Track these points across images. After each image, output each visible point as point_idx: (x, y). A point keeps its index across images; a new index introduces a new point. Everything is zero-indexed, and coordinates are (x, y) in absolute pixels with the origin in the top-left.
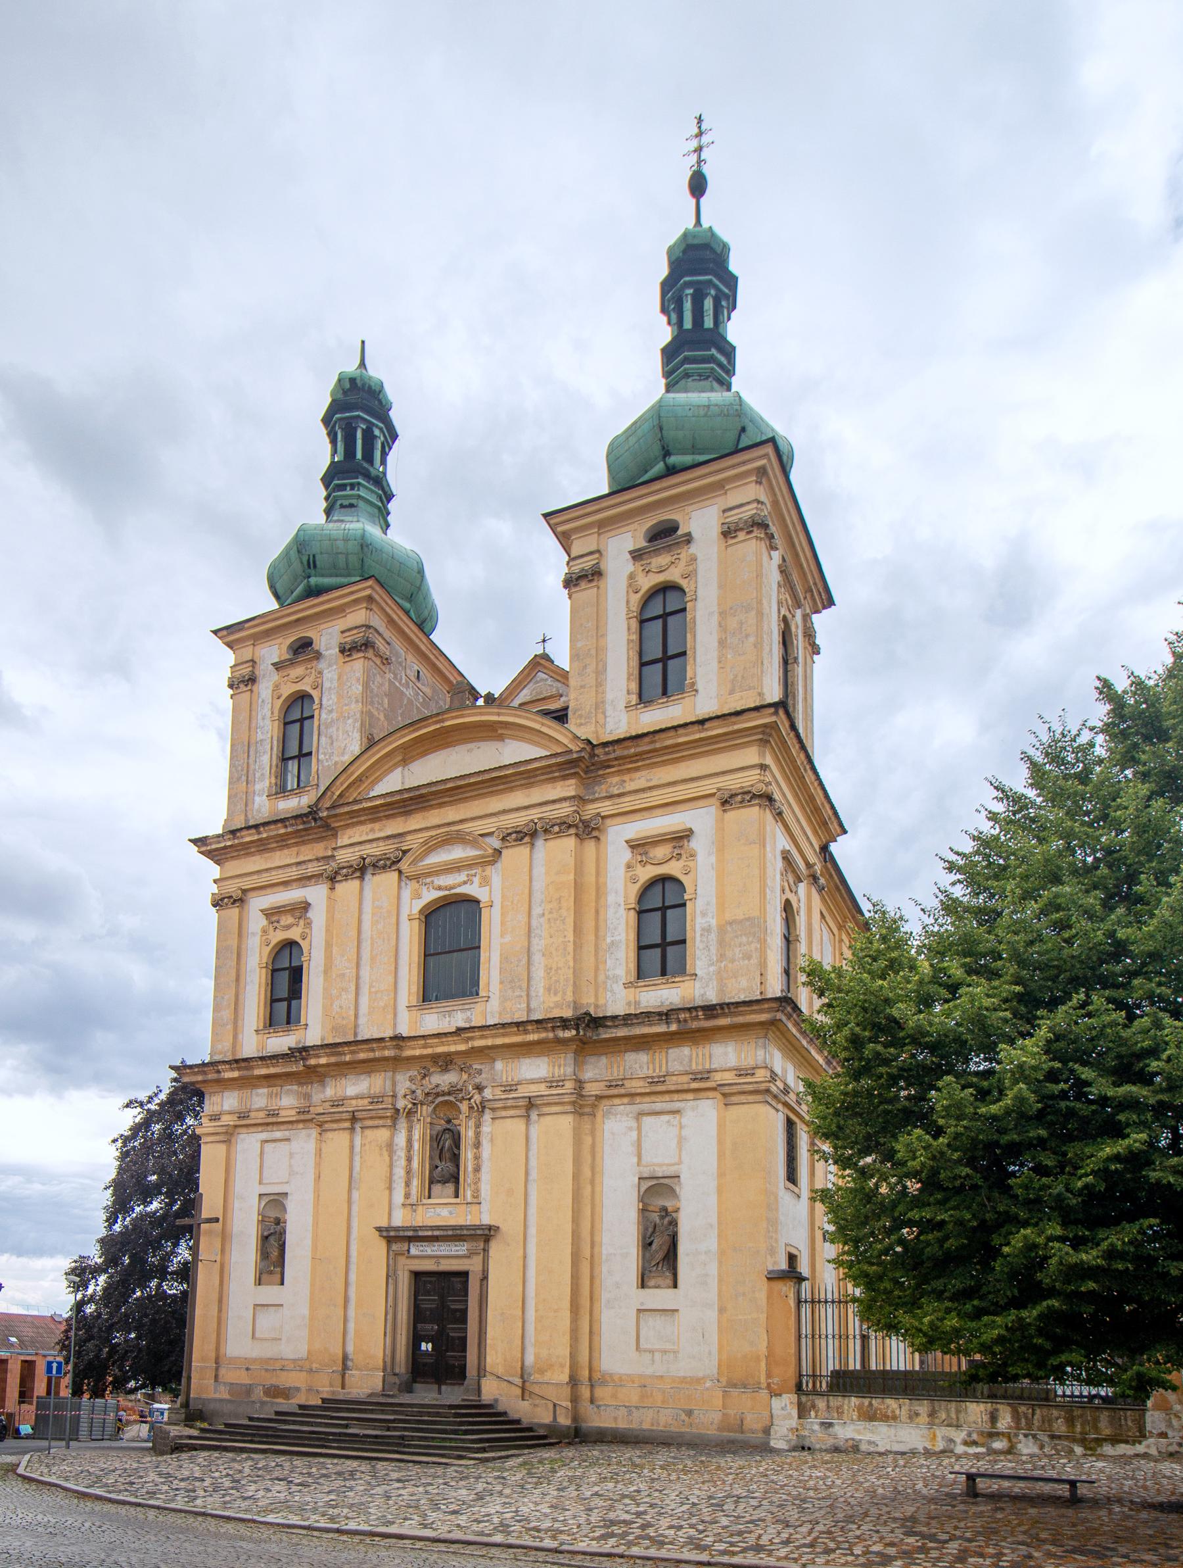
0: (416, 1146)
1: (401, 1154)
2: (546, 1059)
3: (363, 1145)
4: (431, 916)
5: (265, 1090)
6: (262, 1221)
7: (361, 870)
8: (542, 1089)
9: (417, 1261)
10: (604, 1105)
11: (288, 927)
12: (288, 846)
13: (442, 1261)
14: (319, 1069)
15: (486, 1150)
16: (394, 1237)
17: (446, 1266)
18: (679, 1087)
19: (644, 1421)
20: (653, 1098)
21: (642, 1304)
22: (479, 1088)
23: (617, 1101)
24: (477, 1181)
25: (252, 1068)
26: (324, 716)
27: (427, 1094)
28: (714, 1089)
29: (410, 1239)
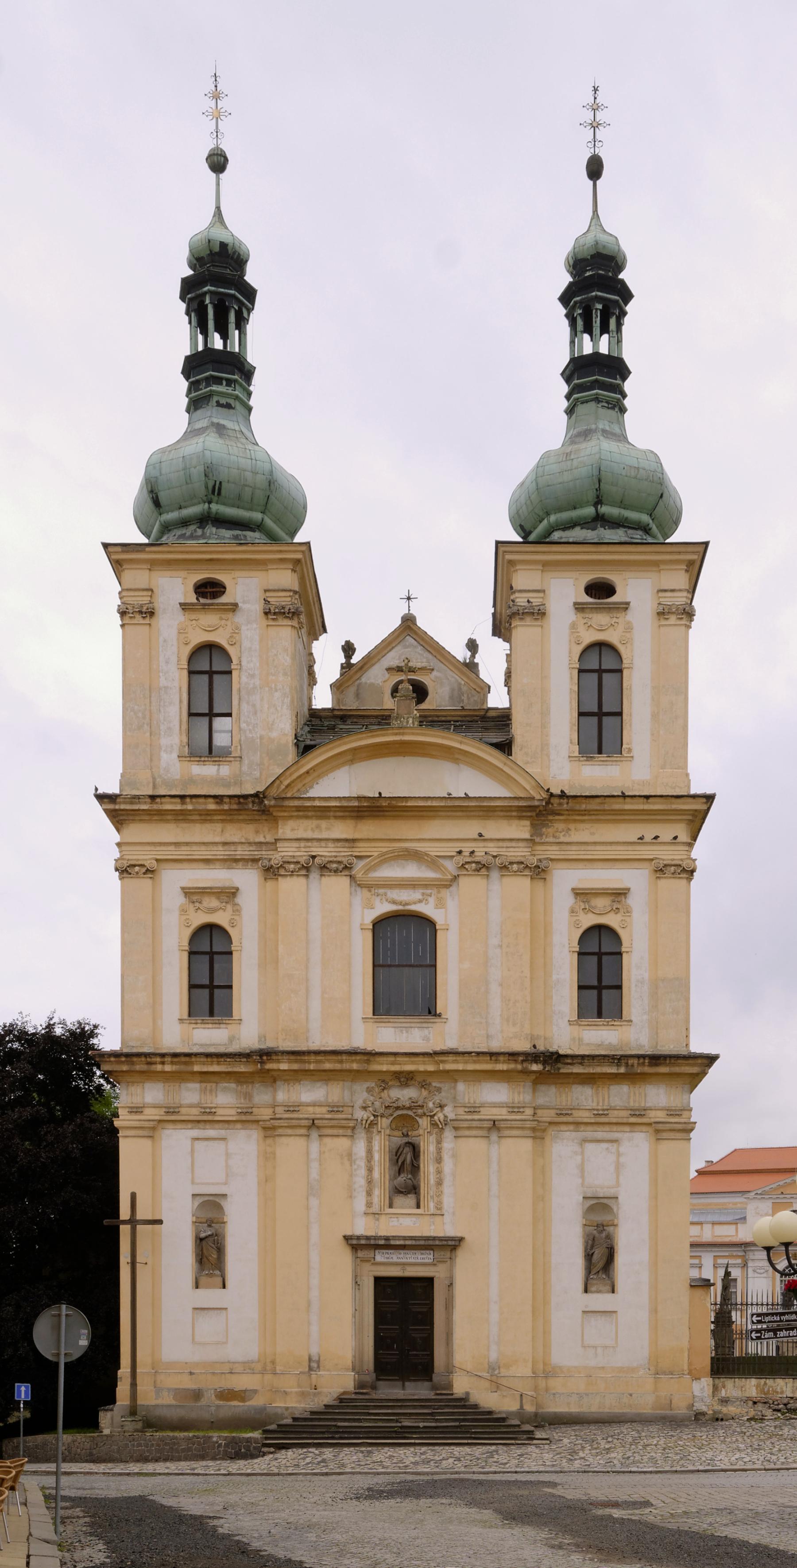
0: (376, 1156)
1: (362, 1163)
2: (505, 1085)
3: (321, 1153)
5: (197, 1085)
7: (306, 868)
8: (501, 1114)
9: (382, 1268)
10: (552, 1131)
11: (212, 911)
12: (211, 821)
13: (409, 1268)
14: (273, 1073)
15: (448, 1166)
17: (410, 1272)
18: (620, 1121)
19: (592, 1406)
20: (596, 1128)
21: (586, 1306)
22: (441, 1107)
23: (563, 1128)
24: (440, 1194)
25: (192, 1063)
26: (244, 679)
27: (387, 1107)
28: (650, 1124)
29: (377, 1247)
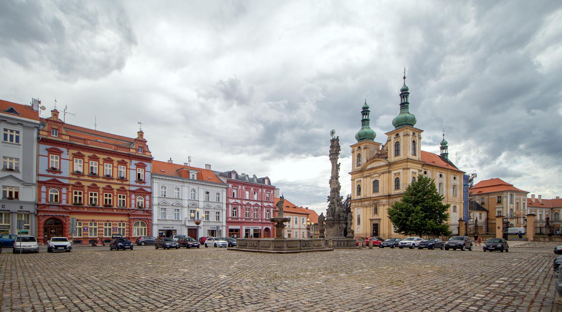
4: (374, 182)
7: (366, 177)
16: (371, 220)
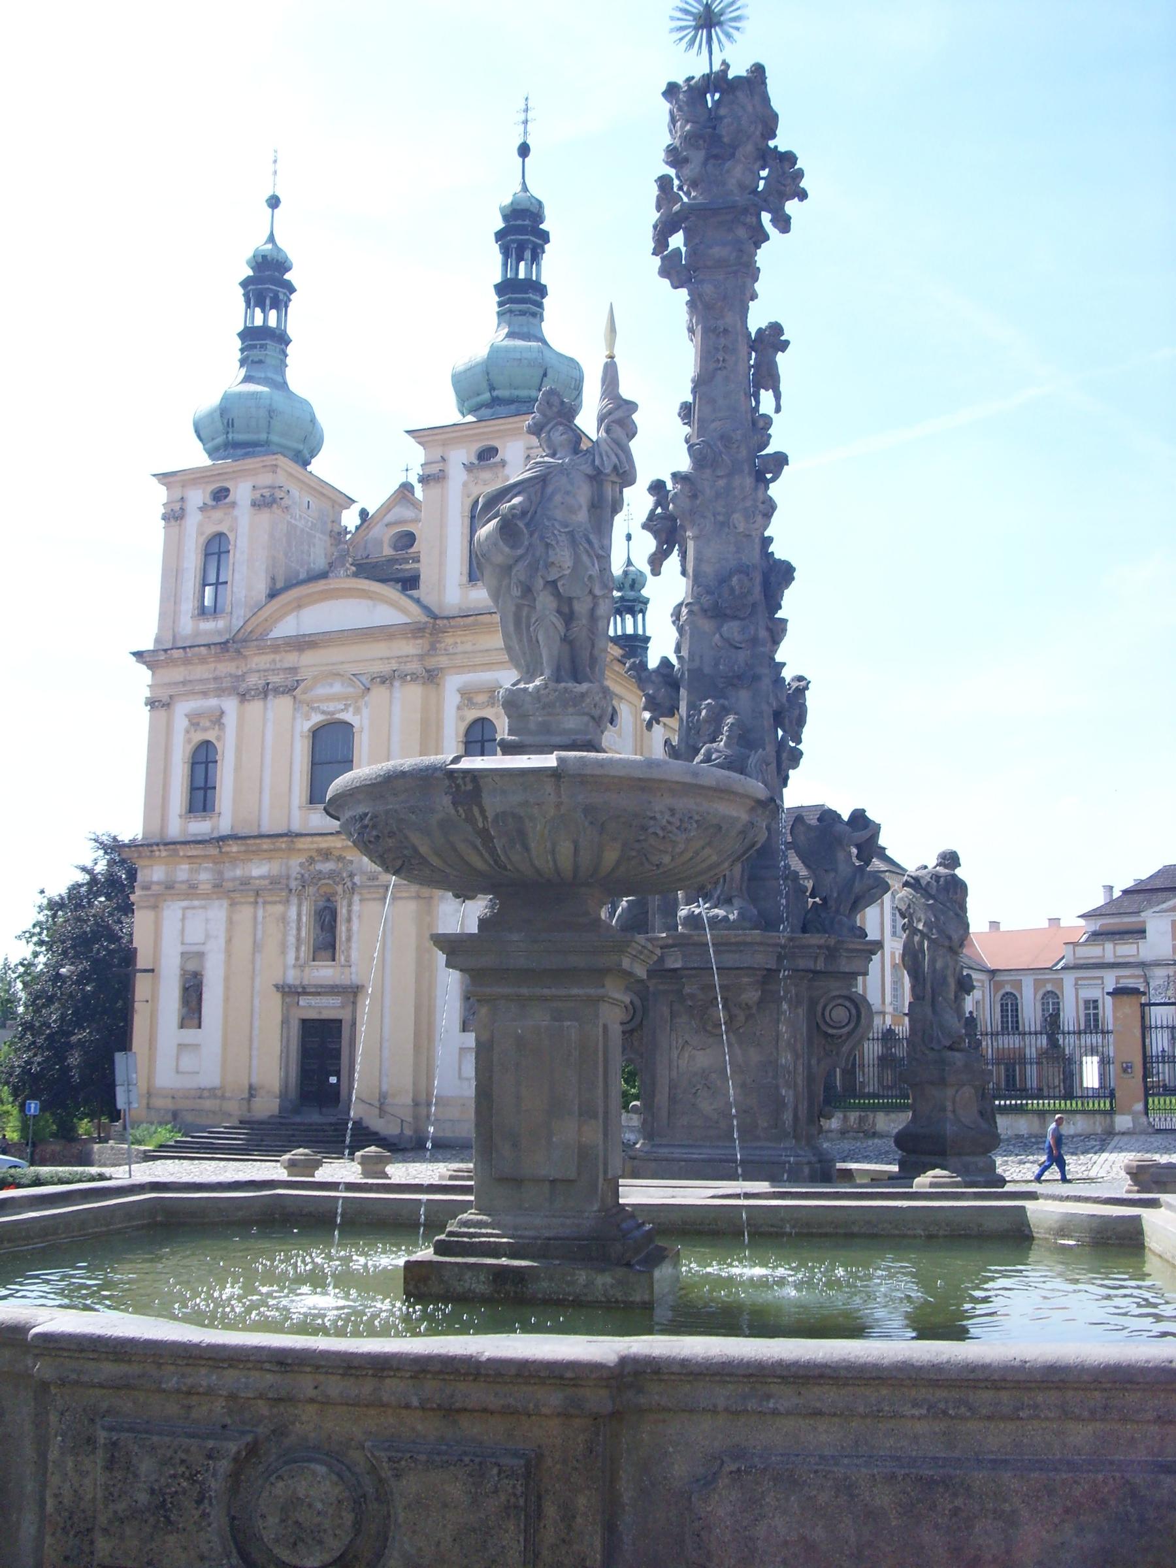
0: (304, 919)
1: (294, 925)
3: (264, 918)
6: (184, 972)
22: (351, 876)
26: (237, 555)
